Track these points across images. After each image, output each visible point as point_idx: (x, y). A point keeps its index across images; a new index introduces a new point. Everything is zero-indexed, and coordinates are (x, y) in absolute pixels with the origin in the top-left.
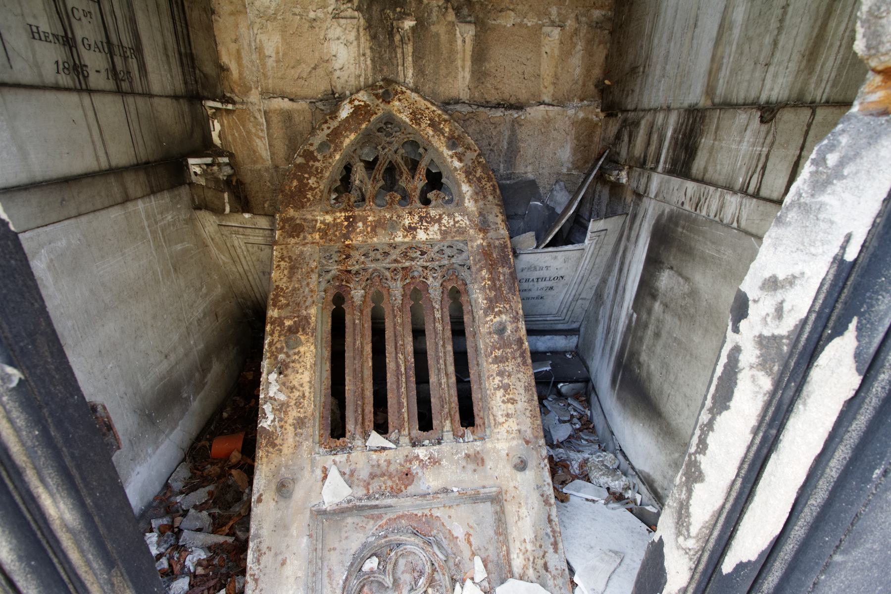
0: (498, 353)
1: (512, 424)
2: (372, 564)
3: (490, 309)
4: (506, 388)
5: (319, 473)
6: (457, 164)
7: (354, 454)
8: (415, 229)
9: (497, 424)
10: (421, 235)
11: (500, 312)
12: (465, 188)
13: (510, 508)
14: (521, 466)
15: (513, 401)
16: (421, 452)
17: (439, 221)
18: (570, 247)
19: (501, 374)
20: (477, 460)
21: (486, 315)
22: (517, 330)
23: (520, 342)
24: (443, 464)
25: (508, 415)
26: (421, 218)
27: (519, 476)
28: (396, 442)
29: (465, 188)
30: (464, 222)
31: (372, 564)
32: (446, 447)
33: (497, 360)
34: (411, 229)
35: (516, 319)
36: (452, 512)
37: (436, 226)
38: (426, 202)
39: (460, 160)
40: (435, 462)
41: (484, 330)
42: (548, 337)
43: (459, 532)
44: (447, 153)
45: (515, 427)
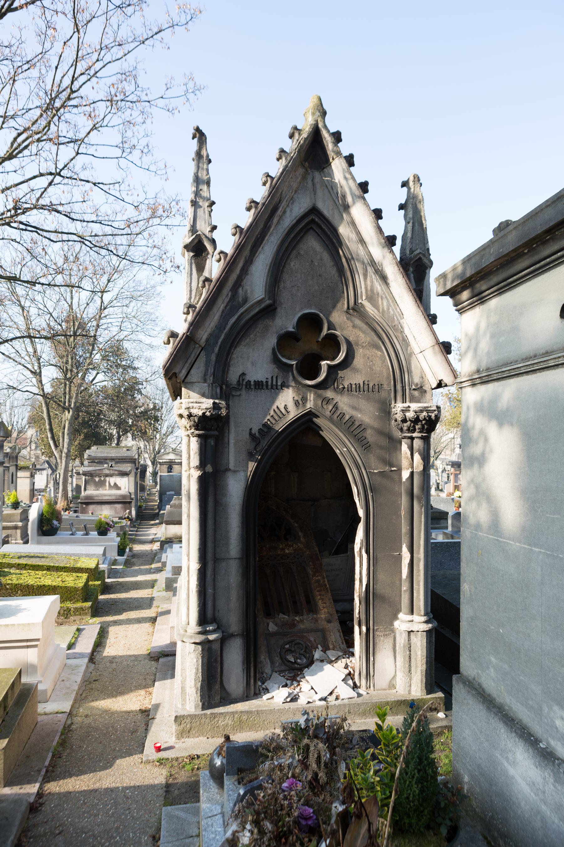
0: (318, 589)
1: (326, 610)
2: (287, 646)
3: (314, 575)
4: (322, 599)
5: (266, 624)
6: (296, 525)
7: (276, 619)
8: (284, 549)
9: (321, 610)
10: (287, 551)
11: (318, 576)
12: (300, 534)
13: (328, 633)
14: (329, 621)
15: (325, 603)
16: (297, 618)
17: (292, 546)
18: (342, 555)
19: (320, 595)
20: (316, 620)
21: (313, 577)
22: (324, 581)
23: (326, 585)
24: (304, 622)
25: (324, 607)
26: (286, 546)
27: (329, 625)
28: (289, 616)
29: (300, 534)
30: (301, 546)
31: (287, 646)
32: (305, 617)
33: (318, 591)
34: (283, 549)
35: (323, 578)
36: (309, 634)
37: (292, 548)
38: (287, 539)
39: (297, 523)
40: (302, 621)
41: (313, 582)
42: (341, 603)
43: (312, 639)
44: (292, 521)
45: (326, 611)
